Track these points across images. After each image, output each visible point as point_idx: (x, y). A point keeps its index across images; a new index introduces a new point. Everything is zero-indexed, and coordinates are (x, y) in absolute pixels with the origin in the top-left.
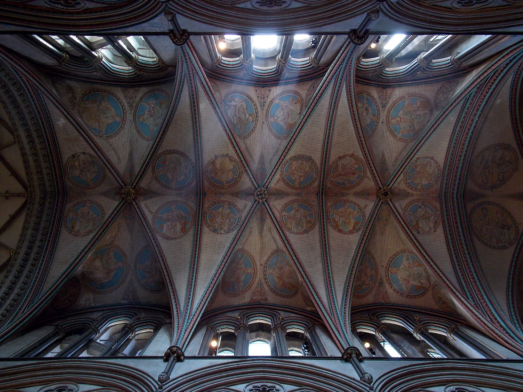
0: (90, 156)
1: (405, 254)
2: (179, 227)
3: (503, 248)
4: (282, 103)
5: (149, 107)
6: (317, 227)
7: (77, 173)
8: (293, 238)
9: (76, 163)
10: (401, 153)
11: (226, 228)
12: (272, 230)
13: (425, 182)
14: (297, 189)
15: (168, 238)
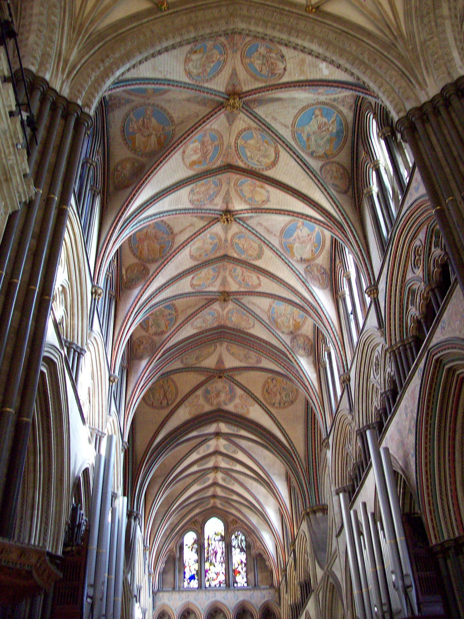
0: (281, 76)
1: (174, 312)
2: (195, 158)
3: (182, 362)
4: (315, 234)
5: (330, 123)
6: (196, 263)
7: (262, 50)
8: (186, 252)
9: (273, 55)
10: (259, 307)
11: (195, 198)
12: (192, 228)
13: (233, 319)
14: (232, 240)
15: (184, 152)
